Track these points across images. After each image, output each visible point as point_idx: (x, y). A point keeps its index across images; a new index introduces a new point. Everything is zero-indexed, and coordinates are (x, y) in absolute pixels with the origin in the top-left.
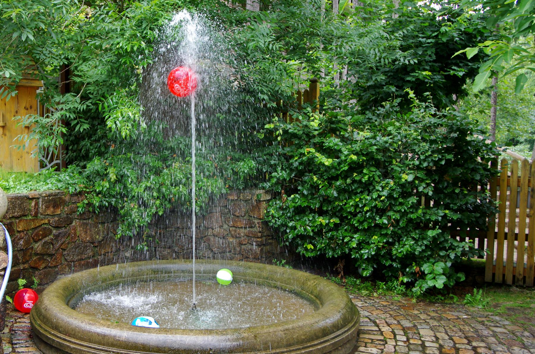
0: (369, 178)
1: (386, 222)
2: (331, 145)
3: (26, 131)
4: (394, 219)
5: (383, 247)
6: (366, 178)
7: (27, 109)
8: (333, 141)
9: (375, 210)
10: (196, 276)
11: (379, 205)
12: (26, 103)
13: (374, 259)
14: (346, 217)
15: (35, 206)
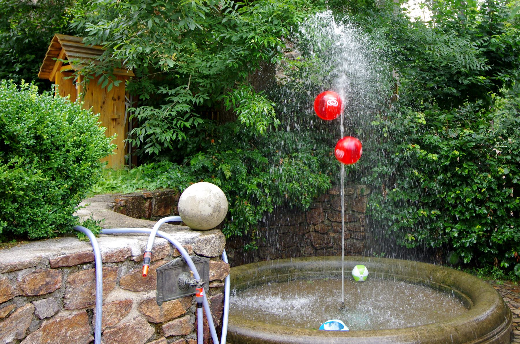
0: (469, 171)
1: (485, 211)
2: (432, 141)
3: (114, 123)
4: (492, 209)
5: (483, 235)
6: (467, 171)
7: (115, 100)
8: (434, 138)
9: (475, 201)
10: (345, 274)
11: (479, 196)
12: (114, 93)
13: (474, 249)
14: (448, 209)
15: (149, 206)
